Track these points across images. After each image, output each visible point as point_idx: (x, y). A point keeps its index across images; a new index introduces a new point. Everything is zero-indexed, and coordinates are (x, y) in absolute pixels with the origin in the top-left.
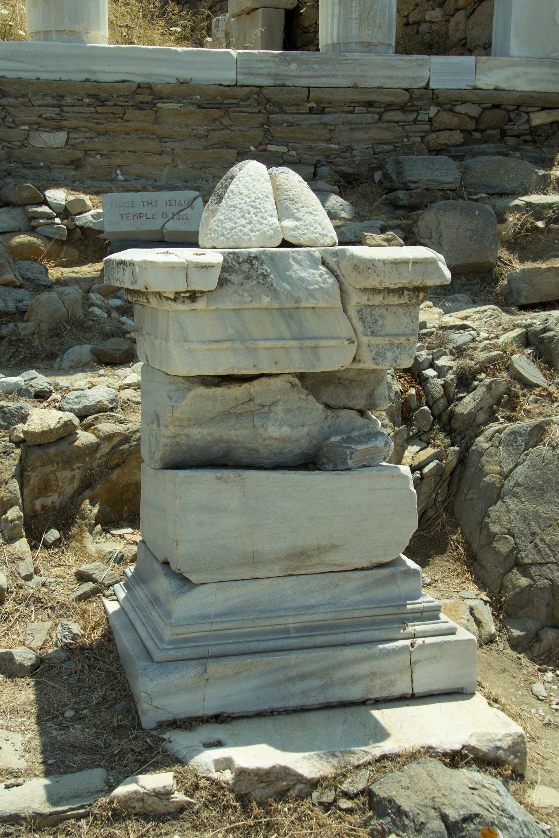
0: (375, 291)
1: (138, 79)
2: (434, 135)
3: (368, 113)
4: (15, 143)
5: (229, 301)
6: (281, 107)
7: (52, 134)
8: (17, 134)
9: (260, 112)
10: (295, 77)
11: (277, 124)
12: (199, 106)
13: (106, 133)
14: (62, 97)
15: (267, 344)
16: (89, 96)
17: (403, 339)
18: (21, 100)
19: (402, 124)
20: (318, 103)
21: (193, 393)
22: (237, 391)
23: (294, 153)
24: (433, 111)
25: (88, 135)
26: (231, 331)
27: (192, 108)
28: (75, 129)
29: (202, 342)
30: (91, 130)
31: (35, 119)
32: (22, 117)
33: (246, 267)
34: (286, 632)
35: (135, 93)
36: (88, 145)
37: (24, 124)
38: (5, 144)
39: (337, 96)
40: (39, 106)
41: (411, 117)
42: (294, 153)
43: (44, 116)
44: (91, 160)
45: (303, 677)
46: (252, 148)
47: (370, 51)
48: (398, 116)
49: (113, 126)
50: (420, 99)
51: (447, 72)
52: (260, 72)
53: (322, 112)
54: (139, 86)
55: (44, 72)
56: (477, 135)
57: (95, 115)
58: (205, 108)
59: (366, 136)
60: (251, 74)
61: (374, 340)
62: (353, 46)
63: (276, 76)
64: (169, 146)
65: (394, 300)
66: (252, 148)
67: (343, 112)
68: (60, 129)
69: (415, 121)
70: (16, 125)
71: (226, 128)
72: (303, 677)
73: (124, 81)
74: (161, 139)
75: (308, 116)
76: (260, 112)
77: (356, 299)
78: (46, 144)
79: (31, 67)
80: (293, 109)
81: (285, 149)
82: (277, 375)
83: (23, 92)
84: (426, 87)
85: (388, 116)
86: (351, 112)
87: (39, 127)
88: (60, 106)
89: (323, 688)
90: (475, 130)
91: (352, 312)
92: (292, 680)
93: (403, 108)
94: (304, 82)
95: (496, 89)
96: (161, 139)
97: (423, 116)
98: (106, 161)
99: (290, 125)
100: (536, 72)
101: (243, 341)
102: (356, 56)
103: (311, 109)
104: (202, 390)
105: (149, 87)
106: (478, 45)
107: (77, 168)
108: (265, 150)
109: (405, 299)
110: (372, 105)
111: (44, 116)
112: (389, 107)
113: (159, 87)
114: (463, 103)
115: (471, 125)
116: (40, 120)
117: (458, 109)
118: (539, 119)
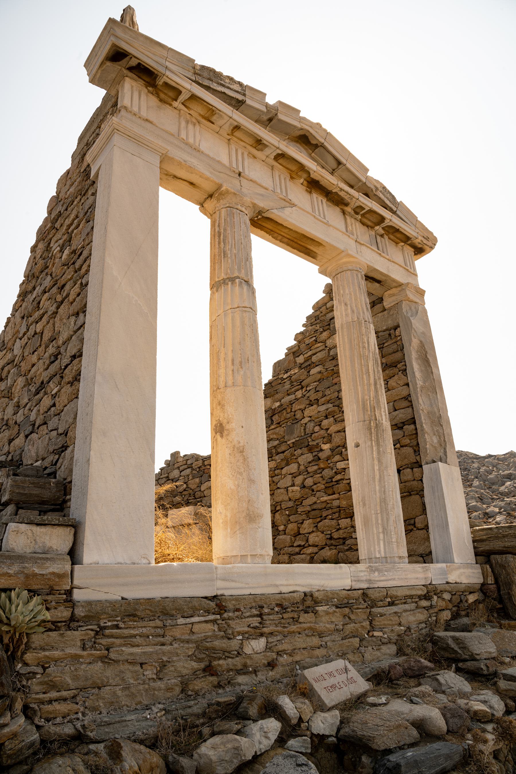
1: (302, 589)
4: (233, 652)
7: (257, 641)
8: (235, 644)
10: (378, 581)
12: (337, 607)
14: (262, 607)
16: (278, 605)
18: (237, 613)
31: (246, 629)
32: (239, 629)
36: (280, 647)
37: (239, 633)
38: (227, 654)
40: (248, 617)
43: (252, 625)
44: (281, 659)
52: (362, 579)
55: (248, 588)
57: (283, 621)
58: (340, 608)
60: (358, 581)
63: (369, 581)
68: (262, 635)
73: (294, 592)
74: (321, 635)
75: (388, 608)
78: (254, 650)
83: (237, 607)
86: (405, 603)
87: (248, 636)
88: (260, 615)
111: (252, 625)
116: (249, 629)
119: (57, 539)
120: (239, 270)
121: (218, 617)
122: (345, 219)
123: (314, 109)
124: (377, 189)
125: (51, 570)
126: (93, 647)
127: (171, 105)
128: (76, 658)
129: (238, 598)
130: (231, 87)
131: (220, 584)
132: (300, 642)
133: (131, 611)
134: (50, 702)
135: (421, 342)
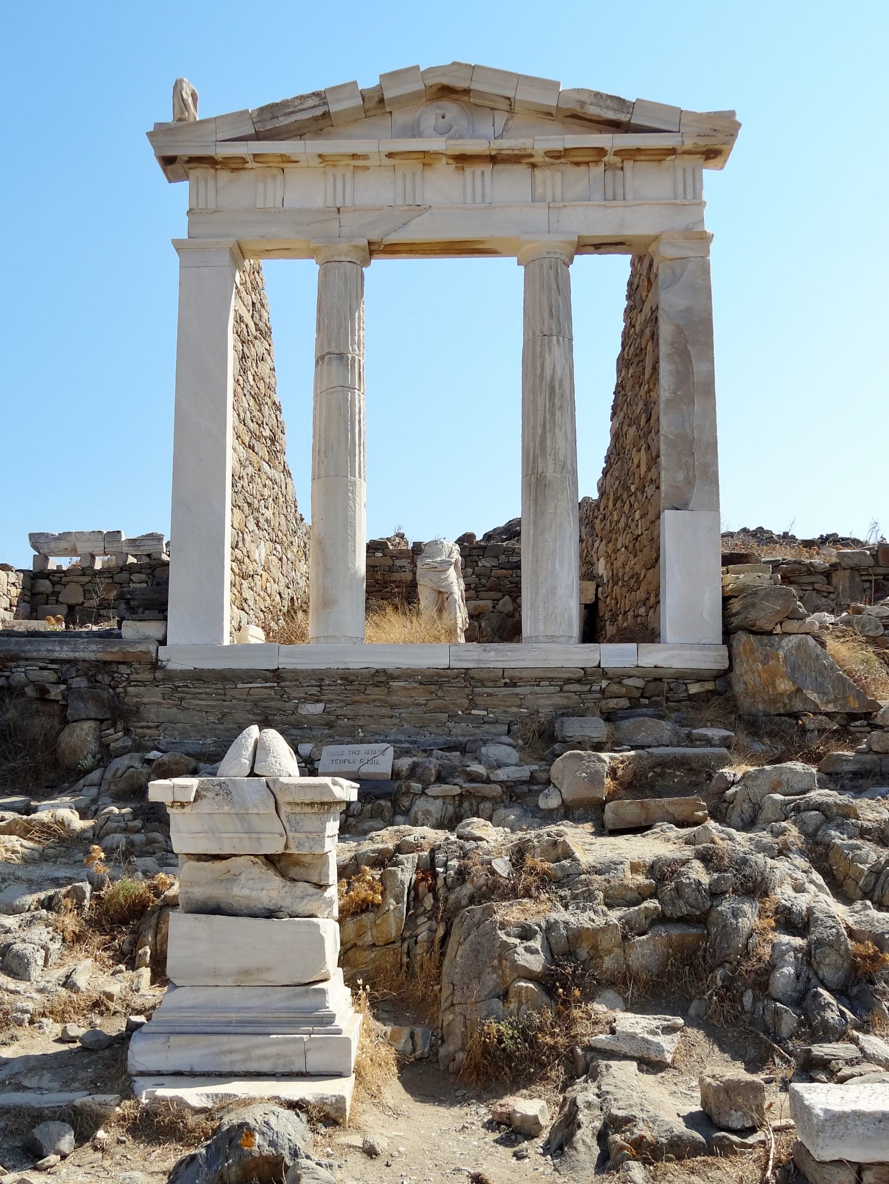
0: (297, 804)
2: (604, 702)
3: (551, 685)
5: (204, 806)
6: (482, 683)
8: (289, 706)
9: (466, 687)
11: (479, 695)
12: (421, 684)
13: (354, 703)
15: (228, 835)
16: (342, 679)
17: (315, 835)
18: (294, 683)
19: (578, 693)
20: (511, 679)
21: (187, 864)
23: (492, 715)
24: (604, 683)
25: (338, 705)
26: (206, 827)
27: (415, 685)
28: (331, 701)
29: (189, 833)
30: (342, 701)
31: (302, 695)
32: (294, 695)
33: (217, 788)
34: (229, 1023)
35: (374, 675)
36: (339, 712)
37: (295, 698)
39: (525, 674)
41: (587, 688)
42: (492, 715)
44: (340, 722)
45: (231, 1052)
46: (460, 712)
47: (554, 642)
48: (577, 687)
49: (357, 698)
50: (592, 675)
51: (615, 655)
53: (515, 685)
54: (377, 671)
56: (645, 701)
59: (550, 703)
61: (297, 835)
62: (541, 639)
64: (396, 712)
65: (308, 810)
66: (460, 712)
67: (531, 685)
70: (289, 699)
71: (440, 698)
72: (231, 1052)
76: (466, 687)
77: (284, 809)
79: (303, 661)
80: (491, 684)
81: (485, 713)
82: (241, 855)
84: (599, 666)
85: (566, 688)
86: (538, 686)
87: (305, 700)
88: (320, 686)
90: (642, 697)
91: (283, 817)
92: (223, 1053)
93: (579, 681)
94: (500, 665)
95: (655, 667)
96: (392, 707)
97: (596, 688)
98: (351, 722)
99: (489, 695)
100: (687, 653)
101: (213, 833)
102: (541, 645)
103: (505, 684)
104: (193, 863)
105: (384, 671)
107: (331, 728)
108: (470, 714)
109: (315, 810)
110: (563, 681)
112: (568, 681)
113: (391, 671)
114: (629, 677)
115: (637, 694)
117: (627, 682)
118: (694, 689)
119: (152, 629)
120: (329, 345)
121: (276, 684)
122: (533, 176)
124: (582, 104)
125: (139, 649)
126: (169, 699)
127: (245, 169)
128: (159, 704)
129: (294, 671)
130: (305, 106)
131: (281, 660)
132: (364, 709)
133: (198, 676)
134: (142, 727)
135: (677, 326)
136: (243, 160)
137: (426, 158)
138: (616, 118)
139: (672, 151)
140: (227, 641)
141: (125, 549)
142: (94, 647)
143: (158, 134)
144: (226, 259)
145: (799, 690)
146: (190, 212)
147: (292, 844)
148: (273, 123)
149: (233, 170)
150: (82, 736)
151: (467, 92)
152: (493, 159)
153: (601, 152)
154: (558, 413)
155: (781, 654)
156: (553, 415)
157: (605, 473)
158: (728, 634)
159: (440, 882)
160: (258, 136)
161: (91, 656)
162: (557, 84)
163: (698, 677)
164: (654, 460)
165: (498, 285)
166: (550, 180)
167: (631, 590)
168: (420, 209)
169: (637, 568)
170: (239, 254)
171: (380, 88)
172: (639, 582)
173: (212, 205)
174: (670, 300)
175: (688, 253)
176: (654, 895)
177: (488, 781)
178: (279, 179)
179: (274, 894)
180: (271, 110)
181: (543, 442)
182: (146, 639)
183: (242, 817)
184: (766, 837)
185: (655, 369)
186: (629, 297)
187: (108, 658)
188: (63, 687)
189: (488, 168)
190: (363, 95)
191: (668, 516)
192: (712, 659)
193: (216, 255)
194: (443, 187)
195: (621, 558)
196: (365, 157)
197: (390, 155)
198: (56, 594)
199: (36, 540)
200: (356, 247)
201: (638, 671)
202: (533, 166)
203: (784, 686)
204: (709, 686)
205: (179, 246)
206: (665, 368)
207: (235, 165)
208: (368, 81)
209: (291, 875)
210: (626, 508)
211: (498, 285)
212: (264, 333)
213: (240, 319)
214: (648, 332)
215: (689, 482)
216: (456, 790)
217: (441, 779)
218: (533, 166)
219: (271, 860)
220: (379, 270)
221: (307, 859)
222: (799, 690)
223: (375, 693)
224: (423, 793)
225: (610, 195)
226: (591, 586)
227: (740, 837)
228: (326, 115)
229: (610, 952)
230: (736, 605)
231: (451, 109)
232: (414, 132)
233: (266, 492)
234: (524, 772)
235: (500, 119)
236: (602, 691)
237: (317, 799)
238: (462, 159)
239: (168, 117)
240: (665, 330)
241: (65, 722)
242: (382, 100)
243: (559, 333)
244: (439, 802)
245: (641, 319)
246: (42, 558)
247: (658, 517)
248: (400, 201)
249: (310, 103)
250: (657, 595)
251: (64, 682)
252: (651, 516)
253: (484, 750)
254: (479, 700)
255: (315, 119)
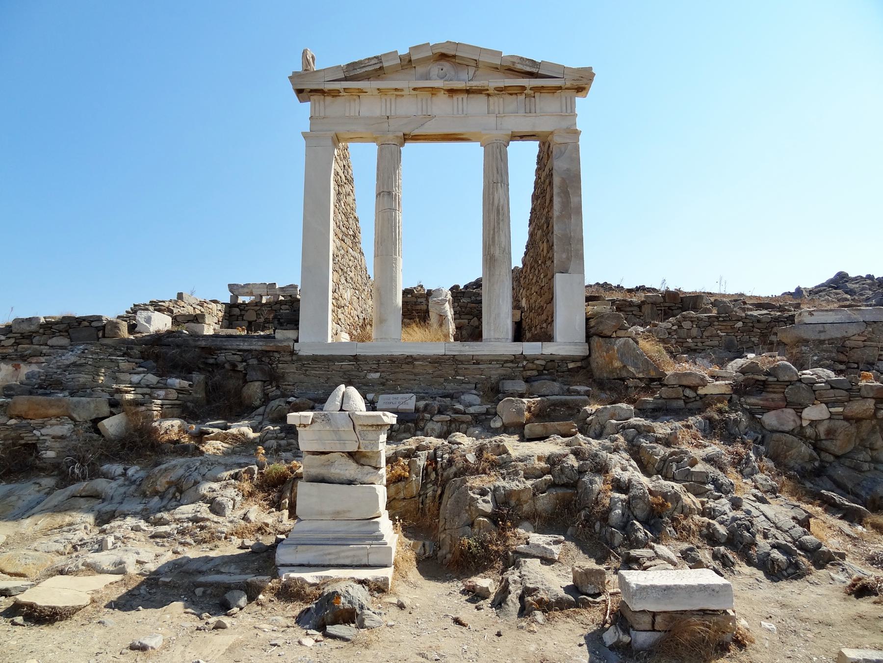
5: (316, 427)
6: (462, 362)
13: (395, 373)
22: (323, 457)
24: (525, 363)
28: (383, 372)
34: (328, 539)
36: (388, 377)
39: (484, 358)
45: (329, 554)
51: (530, 348)
53: (479, 364)
63: (461, 351)
65: (370, 428)
69: (517, 367)
72: (329, 554)
74: (415, 375)
77: (358, 428)
87: (371, 371)
89: (337, 558)
92: (326, 555)
93: (512, 362)
96: (415, 375)
100: (567, 347)
105: (411, 356)
106: (548, 337)
110: (503, 361)
112: (506, 362)
115: (542, 368)
117: (536, 362)
118: (571, 365)
119: (291, 334)
122: (488, 101)
123: (437, 36)
124: (514, 63)
129: (364, 356)
131: (358, 350)
132: (400, 376)
133: (315, 359)
136: (339, 91)
137: (433, 91)
138: (530, 71)
139: (560, 88)
140: (330, 340)
141: (278, 293)
142: (261, 343)
143: (295, 77)
144: (330, 143)
145: (625, 366)
146: (311, 118)
147: (362, 447)
148: (355, 72)
149: (333, 96)
150: (254, 389)
151: (454, 56)
152: (468, 91)
153: (523, 88)
154: (501, 223)
155: (616, 347)
156: (499, 224)
157: (526, 254)
158: (588, 337)
159: (439, 466)
160: (346, 79)
161: (259, 348)
162: (501, 53)
163: (573, 359)
164: (551, 247)
165: (470, 157)
166: (497, 103)
167: (539, 315)
168: (430, 117)
169: (542, 304)
170: (337, 140)
171: (409, 55)
172: (543, 310)
173: (322, 114)
174: (559, 165)
175: (568, 141)
176: (549, 473)
177: (465, 413)
178: (357, 100)
179: (352, 472)
180: (353, 65)
181: (493, 238)
182: (288, 339)
183: (336, 432)
184: (607, 442)
185: (551, 201)
186: (538, 163)
187: (268, 349)
188: (244, 364)
189: (465, 96)
190: (401, 58)
191: (558, 276)
192: (579, 350)
193: (324, 140)
194: (442, 106)
195: (534, 298)
196: (402, 90)
197: (414, 89)
198: (242, 315)
199: (232, 287)
200: (397, 137)
201: (542, 357)
202: (488, 95)
203: (617, 364)
204: (579, 364)
205: (305, 135)
206: (557, 200)
207: (334, 94)
208: (403, 51)
209: (362, 462)
210: (537, 272)
211: (470, 157)
212: (350, 181)
213: (337, 174)
214: (547, 181)
215: (569, 259)
216: (448, 418)
217: (440, 412)
218: (488, 95)
219: (351, 455)
220: (409, 148)
221: (370, 454)
222: (625, 366)
223: (406, 367)
224: (431, 419)
225: (528, 111)
226: (518, 312)
227: (594, 442)
228: (381, 68)
229: (527, 502)
230: (592, 323)
231: (446, 66)
232: (427, 77)
233: (351, 263)
234: (483, 409)
235: (471, 71)
236: (524, 367)
237: (375, 423)
238: (452, 92)
239: (299, 69)
240: (556, 180)
241: (246, 382)
242: (410, 61)
243: (502, 182)
244: (439, 424)
245: (544, 174)
246: (235, 297)
247: (553, 277)
248: (420, 113)
249: (373, 62)
250: (552, 317)
251: (245, 361)
252: (549, 276)
253: (462, 397)
254: (460, 371)
255: (376, 70)
